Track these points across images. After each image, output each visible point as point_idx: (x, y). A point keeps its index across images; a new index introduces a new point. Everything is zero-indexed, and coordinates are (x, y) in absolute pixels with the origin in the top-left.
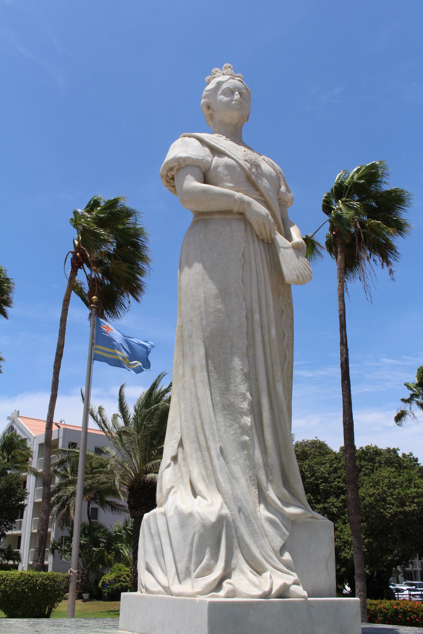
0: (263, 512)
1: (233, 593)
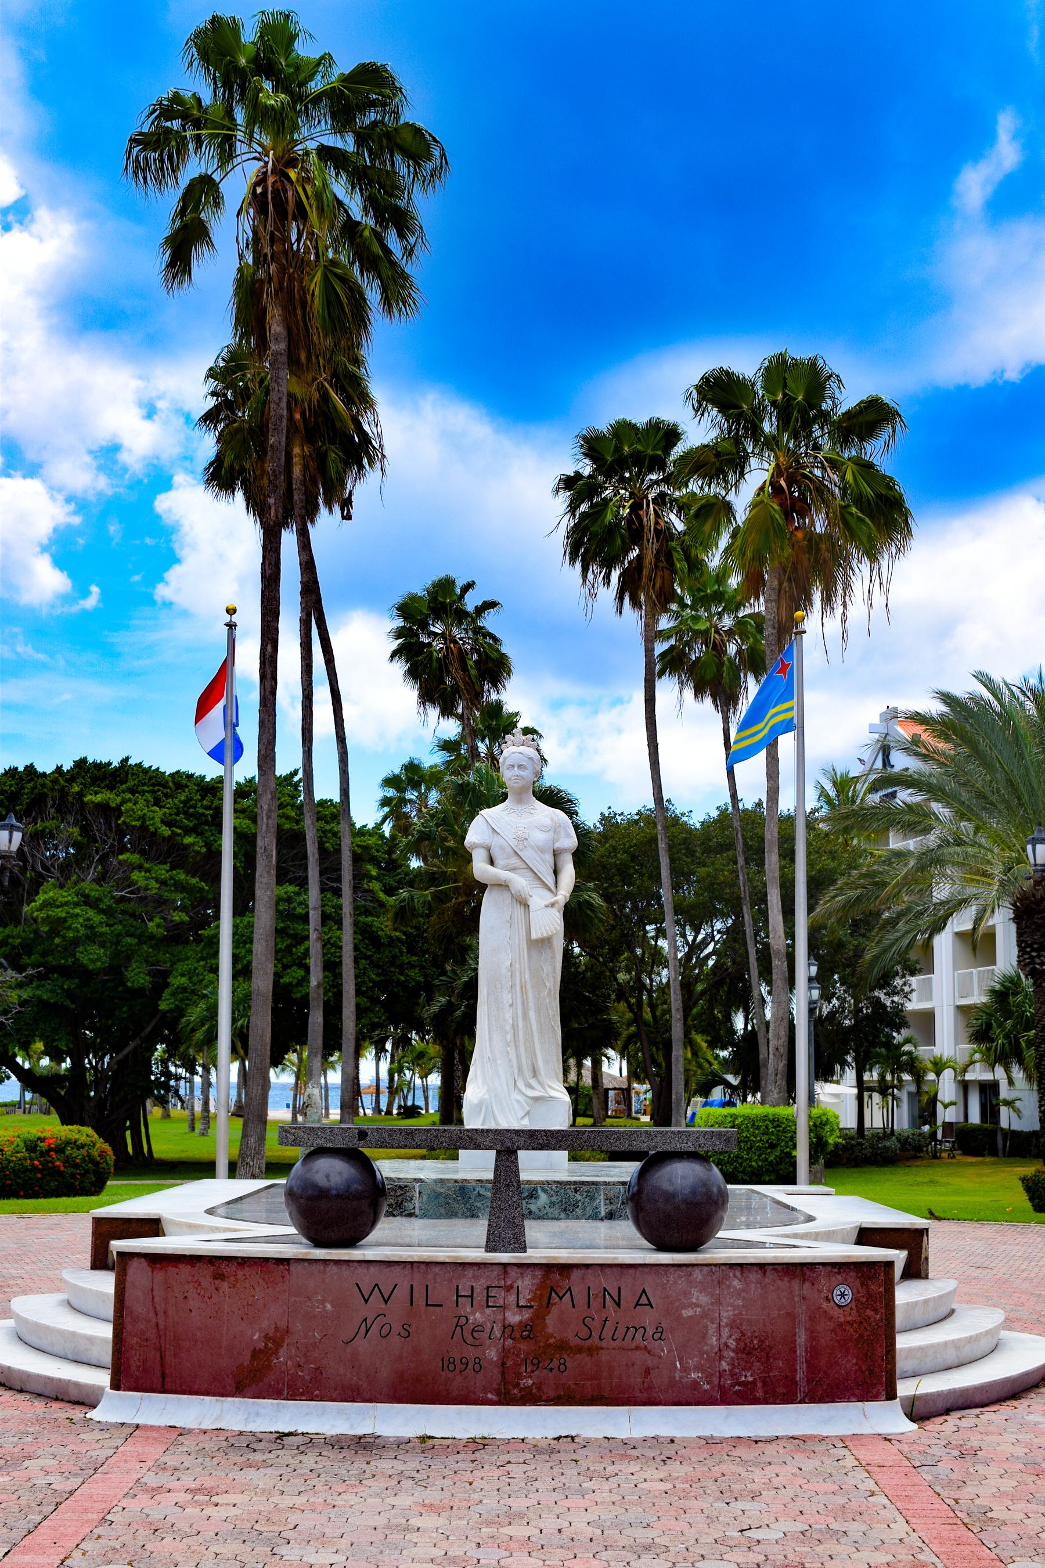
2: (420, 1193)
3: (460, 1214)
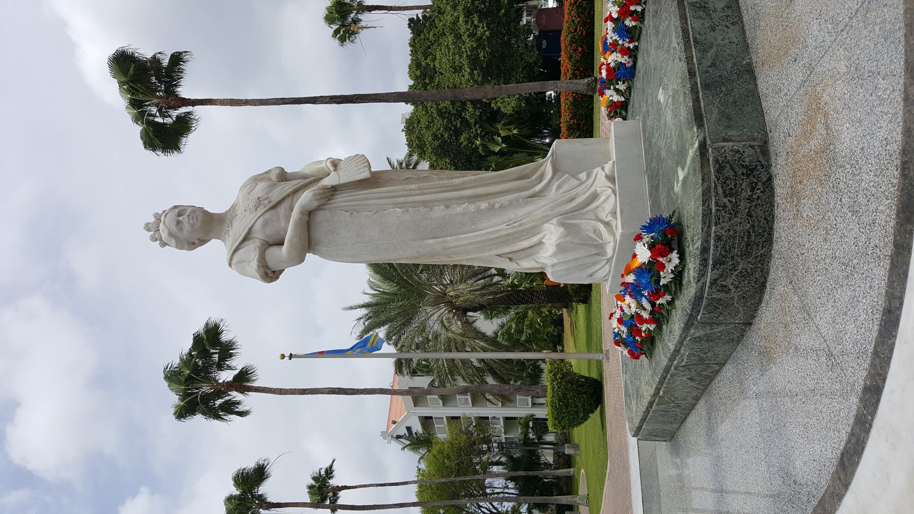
0: (552, 193)
1: (614, 213)
2: (725, 140)
3: (751, 87)
